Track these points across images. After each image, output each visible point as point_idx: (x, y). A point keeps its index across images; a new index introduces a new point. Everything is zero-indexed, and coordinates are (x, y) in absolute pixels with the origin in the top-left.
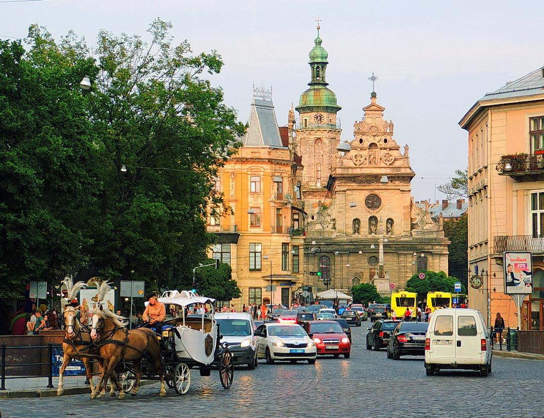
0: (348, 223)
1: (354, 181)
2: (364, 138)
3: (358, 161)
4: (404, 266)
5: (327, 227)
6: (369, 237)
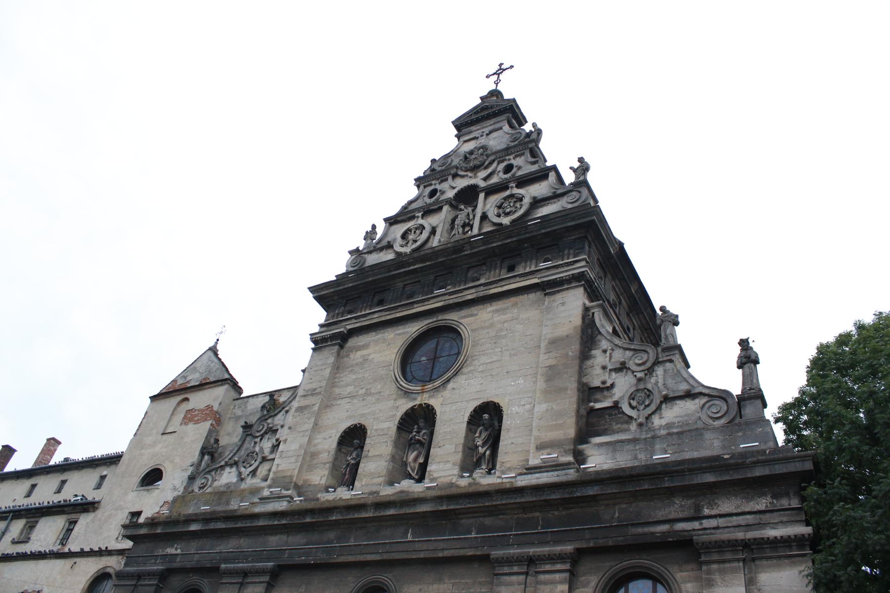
0: (320, 447)
1: (381, 303)
3: (411, 242)
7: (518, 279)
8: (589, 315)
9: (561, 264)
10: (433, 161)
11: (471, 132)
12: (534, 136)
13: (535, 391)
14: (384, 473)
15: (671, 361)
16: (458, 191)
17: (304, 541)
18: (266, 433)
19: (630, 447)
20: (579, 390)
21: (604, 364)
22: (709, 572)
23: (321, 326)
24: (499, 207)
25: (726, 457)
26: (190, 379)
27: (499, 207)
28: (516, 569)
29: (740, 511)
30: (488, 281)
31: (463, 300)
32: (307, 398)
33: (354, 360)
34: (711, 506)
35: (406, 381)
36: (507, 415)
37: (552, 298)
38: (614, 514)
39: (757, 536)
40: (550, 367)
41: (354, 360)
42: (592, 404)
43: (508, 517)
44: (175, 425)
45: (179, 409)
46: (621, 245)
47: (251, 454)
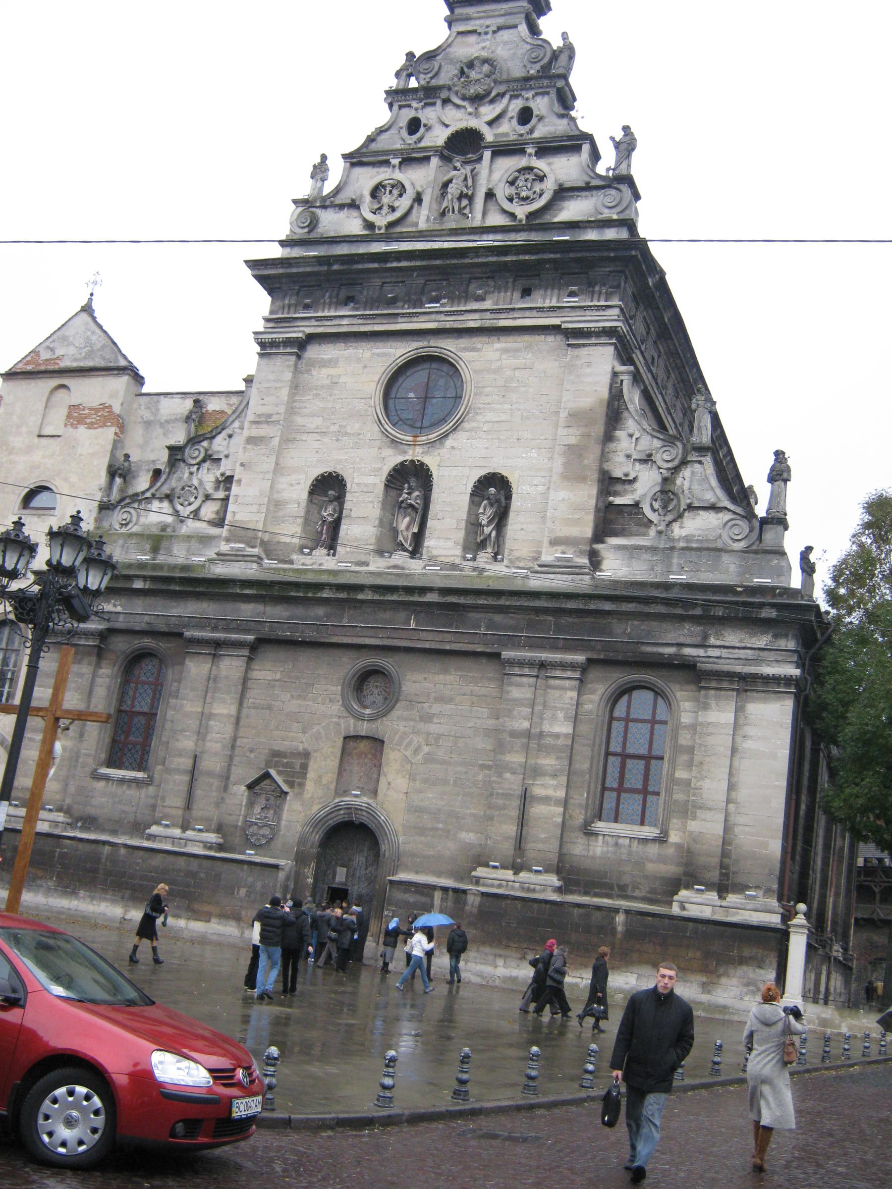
0: (285, 495)
1: (349, 300)
2: (428, 115)
3: (385, 209)
4: (528, 734)
5: (196, 514)
6: (372, 568)
7: (534, 313)
8: (617, 383)
9: (590, 306)
10: (410, 55)
11: (468, 19)
12: (563, 58)
13: (551, 470)
14: (373, 540)
15: (700, 462)
16: (452, 134)
17: (286, 614)
18: (204, 461)
19: (647, 556)
20: (599, 481)
21: (629, 452)
22: (706, 697)
23: (267, 320)
24: (512, 183)
25: (739, 589)
26: (62, 353)
27: (512, 183)
28: (526, 671)
29: (743, 645)
30: (495, 307)
31: (464, 326)
32: (261, 426)
33: (317, 380)
34: (718, 636)
35: (388, 417)
36: (518, 493)
37: (576, 352)
38: (626, 629)
39: (753, 672)
40: (569, 446)
41: (317, 380)
42: (611, 499)
43: (520, 616)
44: (56, 422)
45: (53, 399)
46: (662, 274)
47: (187, 488)
